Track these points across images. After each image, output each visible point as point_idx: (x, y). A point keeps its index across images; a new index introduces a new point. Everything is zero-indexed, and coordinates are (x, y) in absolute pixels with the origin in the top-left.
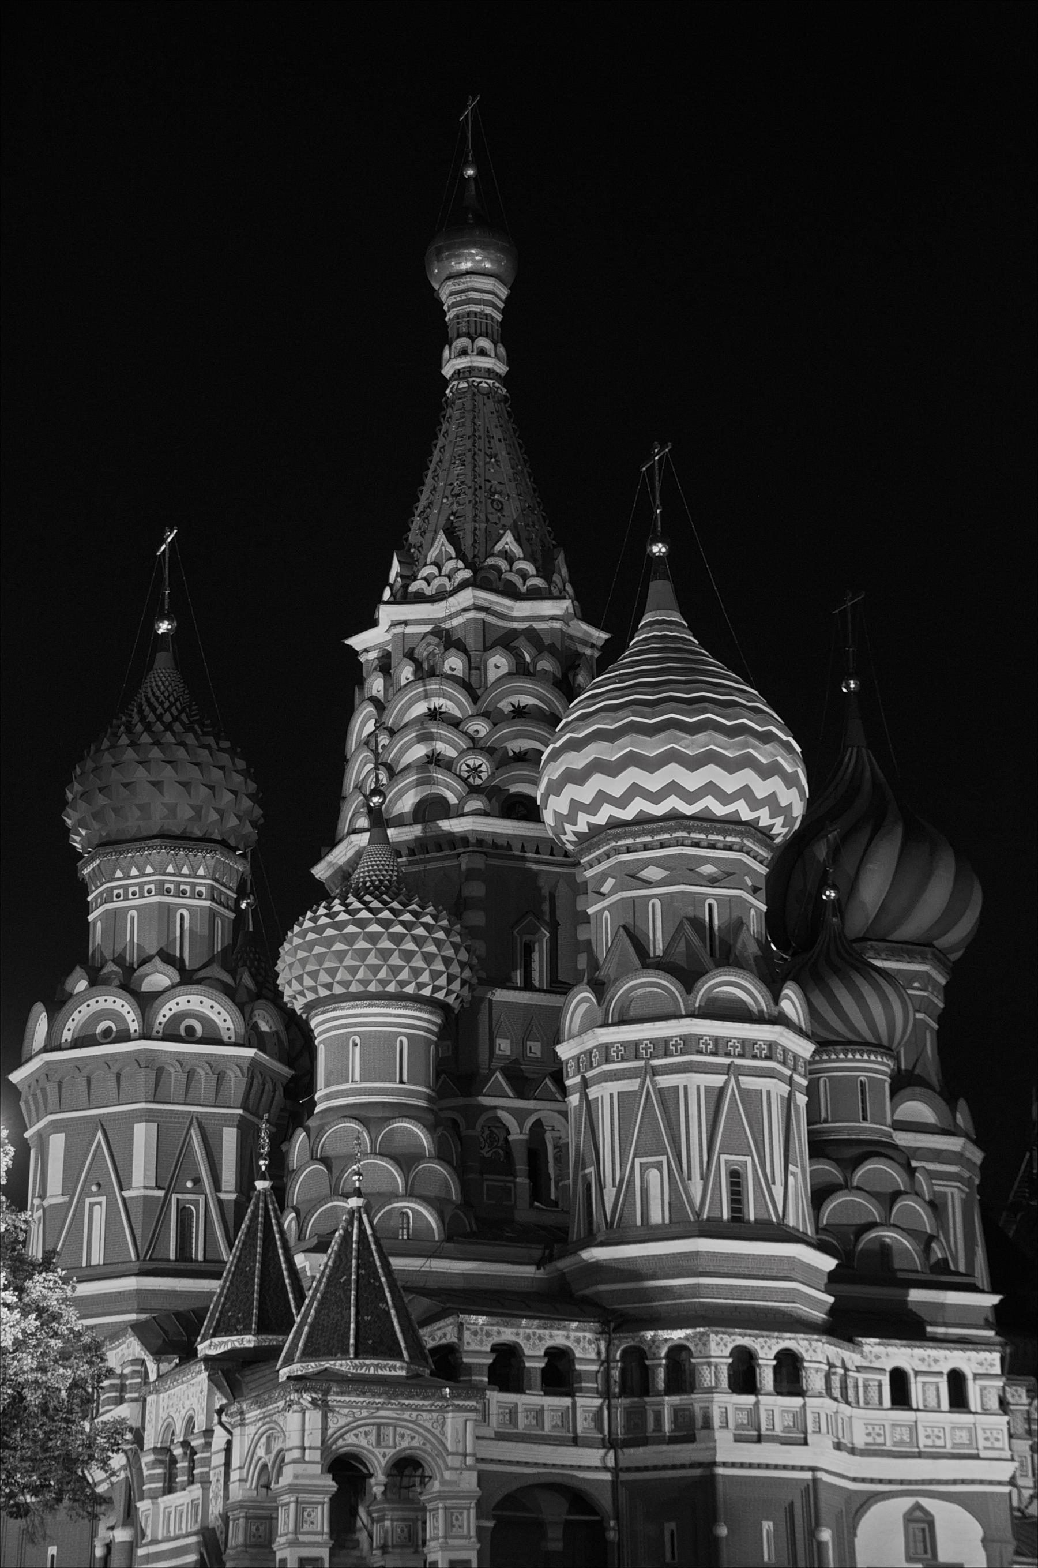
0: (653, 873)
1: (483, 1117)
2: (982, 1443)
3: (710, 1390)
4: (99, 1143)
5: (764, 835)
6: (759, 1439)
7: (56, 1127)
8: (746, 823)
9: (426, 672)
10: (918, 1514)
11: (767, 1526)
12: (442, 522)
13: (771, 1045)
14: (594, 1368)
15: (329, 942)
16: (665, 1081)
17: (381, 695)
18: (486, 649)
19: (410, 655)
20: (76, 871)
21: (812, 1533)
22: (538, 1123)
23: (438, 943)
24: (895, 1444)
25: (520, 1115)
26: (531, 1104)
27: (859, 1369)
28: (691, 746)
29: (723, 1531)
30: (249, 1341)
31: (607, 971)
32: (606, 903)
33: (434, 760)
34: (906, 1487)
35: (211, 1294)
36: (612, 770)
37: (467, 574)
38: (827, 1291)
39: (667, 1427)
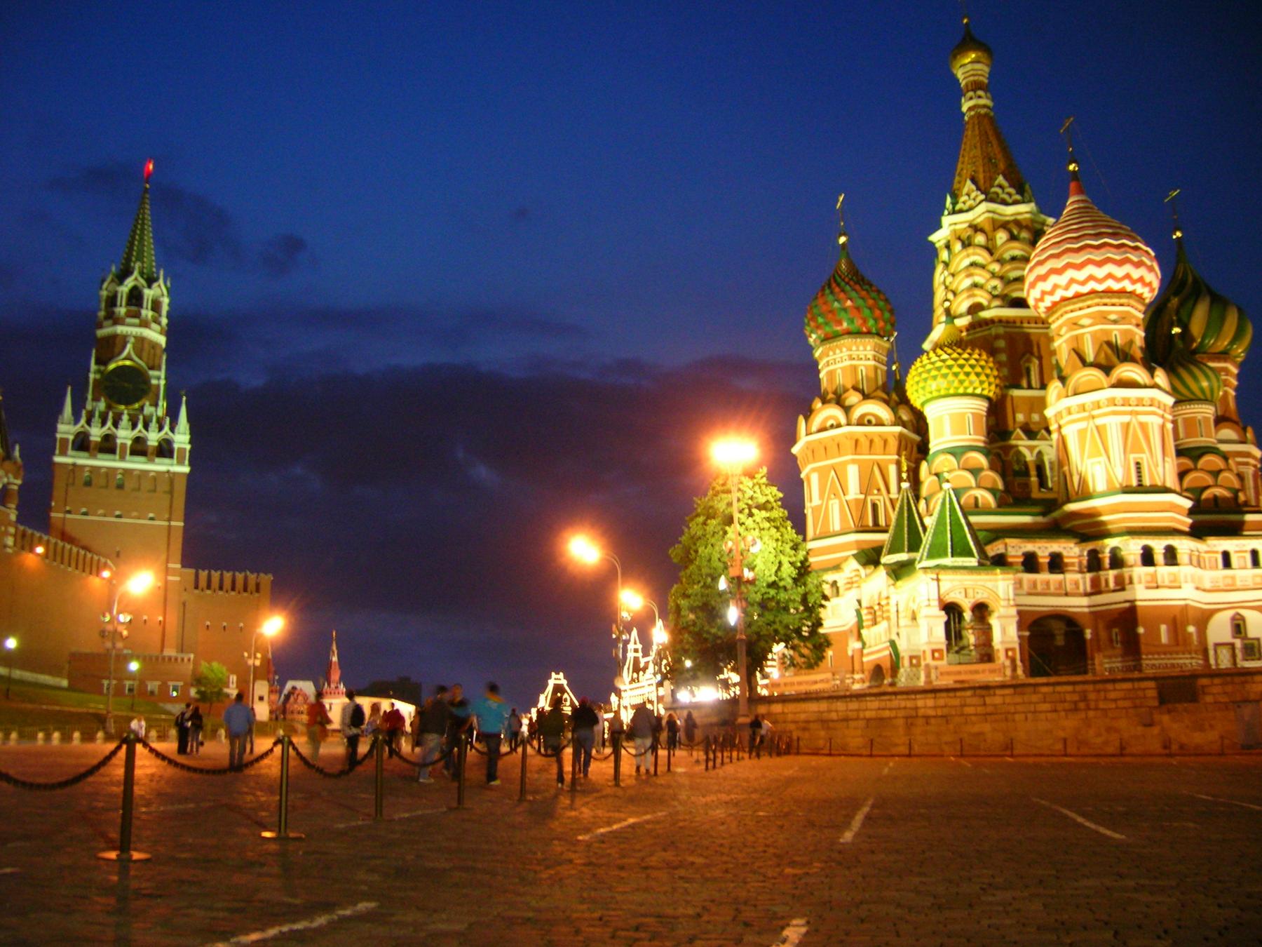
1: (1012, 453)
3: (1131, 566)
4: (833, 478)
5: (1140, 298)
6: (1157, 587)
7: (814, 470)
8: (1130, 292)
9: (967, 244)
10: (1238, 617)
11: (1163, 628)
12: (968, 175)
13: (1152, 400)
18: (995, 229)
19: (959, 238)
20: (812, 355)
24: (1226, 586)
27: (1207, 552)
29: (1141, 630)
33: (975, 285)
34: (1231, 605)
39: (1112, 585)
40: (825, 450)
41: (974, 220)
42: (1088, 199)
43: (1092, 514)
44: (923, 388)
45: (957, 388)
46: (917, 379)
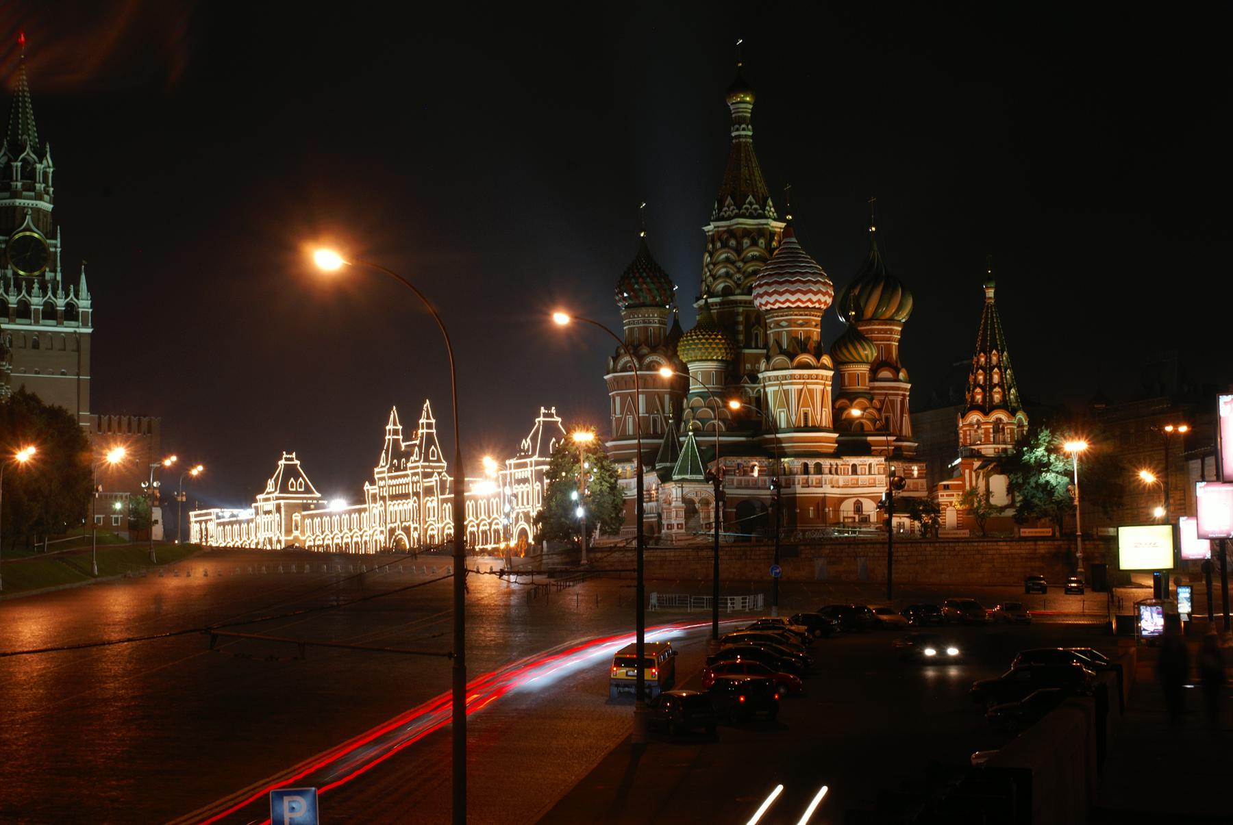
0: (784, 324)
6: (809, 487)
11: (811, 508)
13: (817, 375)
14: (765, 468)
17: (711, 250)
18: (743, 237)
19: (720, 239)
21: (824, 510)
23: (723, 344)
27: (842, 465)
28: (793, 288)
29: (798, 511)
32: (771, 331)
34: (855, 495)
35: (661, 444)
36: (770, 295)
37: (736, 211)
42: (794, 240)
43: (779, 441)
45: (707, 356)
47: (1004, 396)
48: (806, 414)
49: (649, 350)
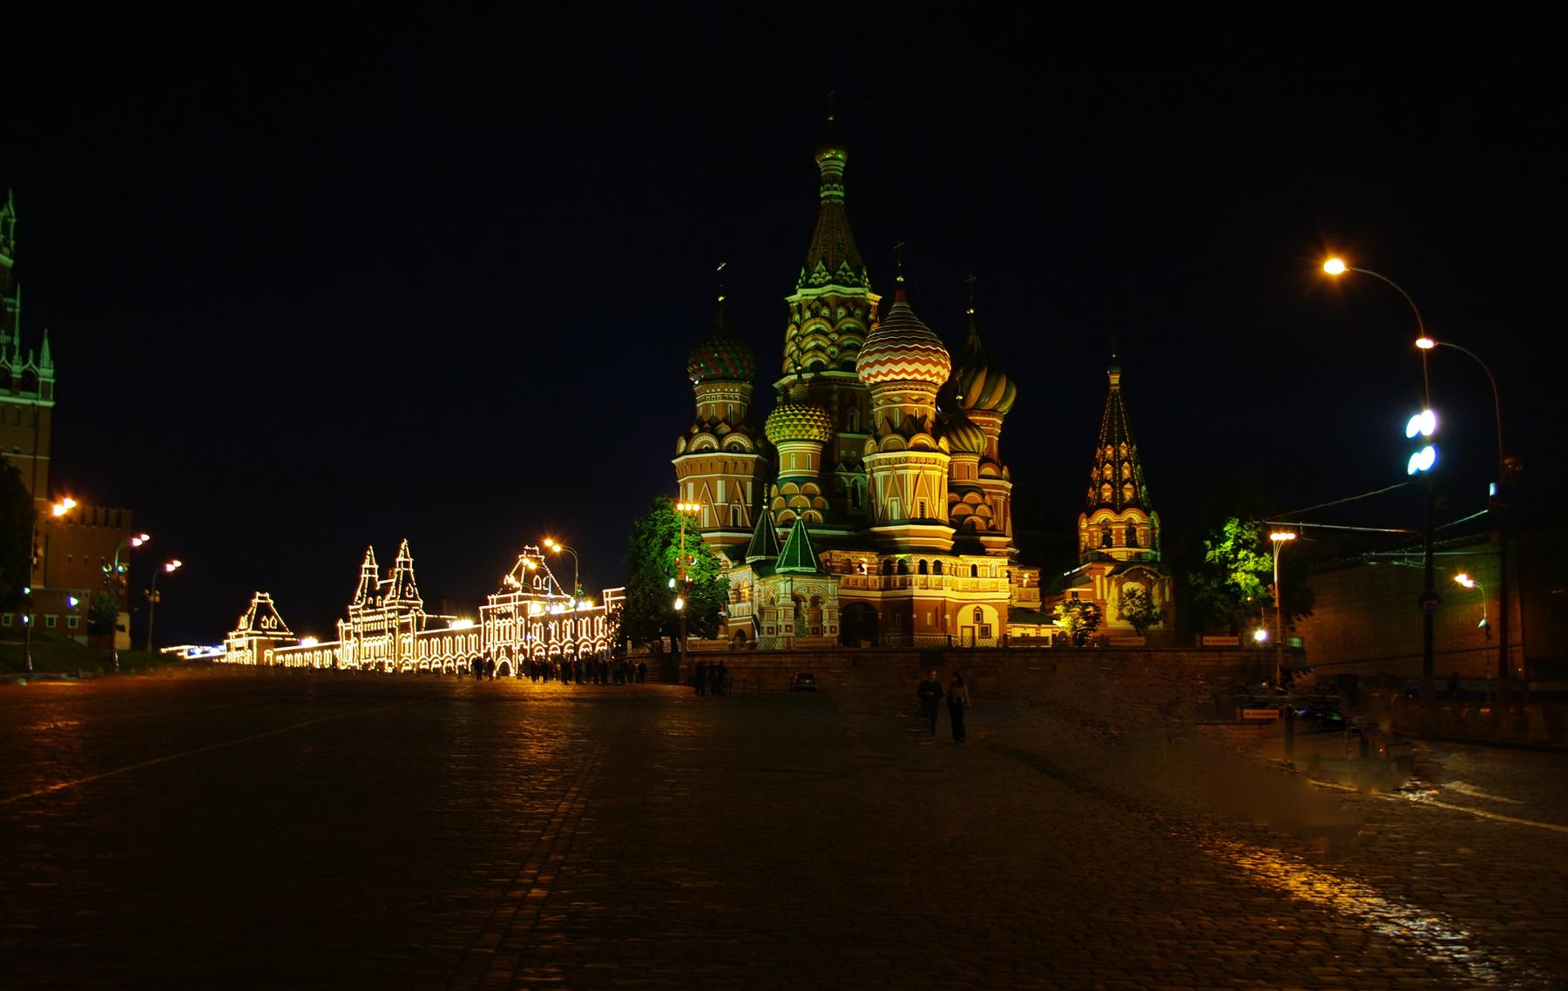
2: (1000, 587)
3: (912, 573)
5: (936, 384)
6: (927, 588)
8: (929, 382)
11: (929, 614)
13: (935, 460)
15: (784, 421)
16: (899, 472)
19: (809, 308)
21: (943, 616)
22: (855, 480)
23: (822, 422)
25: (849, 478)
26: (853, 474)
29: (915, 616)
30: (763, 558)
31: (881, 432)
32: (880, 408)
34: (974, 601)
36: (883, 364)
37: (829, 277)
38: (952, 540)
39: (898, 584)
40: (703, 467)
41: (821, 294)
42: (906, 305)
43: (890, 535)
44: (779, 432)
45: (803, 436)
46: (773, 420)
47: (1135, 494)
48: (922, 504)
49: (730, 429)
